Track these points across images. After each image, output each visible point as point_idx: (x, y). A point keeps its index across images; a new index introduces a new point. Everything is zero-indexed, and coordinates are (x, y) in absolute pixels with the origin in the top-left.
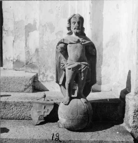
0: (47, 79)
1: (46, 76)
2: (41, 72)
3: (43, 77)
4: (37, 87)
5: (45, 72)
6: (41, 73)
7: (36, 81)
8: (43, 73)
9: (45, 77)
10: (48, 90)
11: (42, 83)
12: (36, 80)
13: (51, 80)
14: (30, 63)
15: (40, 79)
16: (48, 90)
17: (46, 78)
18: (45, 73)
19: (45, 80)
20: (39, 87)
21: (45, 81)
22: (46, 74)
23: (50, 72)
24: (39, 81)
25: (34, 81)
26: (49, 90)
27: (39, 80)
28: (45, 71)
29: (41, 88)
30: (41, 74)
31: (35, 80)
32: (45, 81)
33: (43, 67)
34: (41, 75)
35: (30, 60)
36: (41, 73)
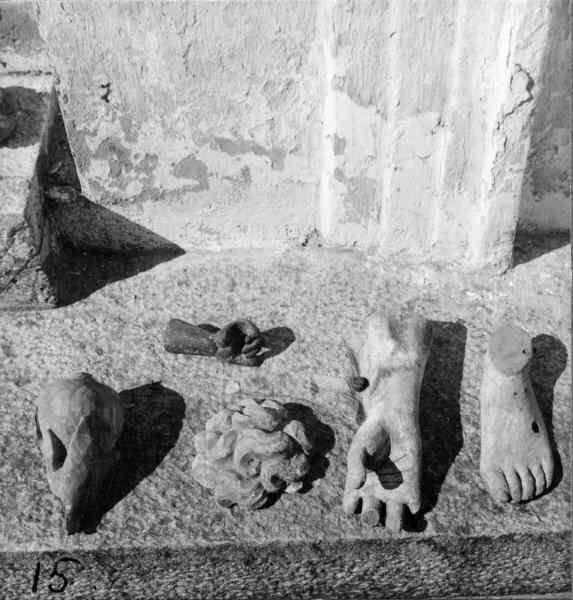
0: (149, 180)
1: (136, 162)
4: (79, 235)
5: (122, 135)
7: (65, 204)
9: (133, 174)
10: (174, 251)
11: (115, 209)
12: (65, 197)
13: (185, 189)
15: (94, 184)
16: (174, 251)
17: (142, 175)
18: (125, 145)
19: (132, 189)
20: (96, 236)
21: (139, 199)
22: (137, 149)
23: (170, 132)
24: (88, 203)
26: (182, 245)
27: (87, 191)
28: (127, 131)
29: (116, 238)
30: (95, 156)
32: (139, 199)
33: (97, 99)
34: (94, 163)
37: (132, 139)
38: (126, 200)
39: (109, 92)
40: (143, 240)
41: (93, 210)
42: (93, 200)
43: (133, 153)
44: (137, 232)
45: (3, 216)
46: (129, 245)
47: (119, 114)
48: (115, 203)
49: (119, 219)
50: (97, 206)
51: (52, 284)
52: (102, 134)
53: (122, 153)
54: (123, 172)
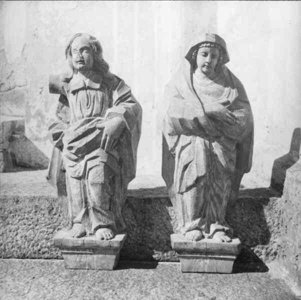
2: (32, 108)
3: (39, 126)
6: (33, 112)
7: (17, 139)
8: (39, 114)
11: (36, 143)
12: (18, 136)
14: (7, 86)
18: (44, 113)
25: (11, 139)
27: (27, 134)
30: (34, 117)
31: (15, 136)
34: (32, 120)
35: (8, 78)
36: (33, 112)
37: (47, 111)
38: (41, 139)
39: (42, 90)
40: (44, 161)
41: (28, 143)
42: (28, 137)
43: (47, 117)
44: (42, 157)
45: (4, 200)
46: (38, 164)
47: (44, 100)
48: (36, 140)
49: (36, 149)
50: (29, 141)
51: (4, 161)
52: (37, 108)
53: (42, 117)
54: (41, 126)
